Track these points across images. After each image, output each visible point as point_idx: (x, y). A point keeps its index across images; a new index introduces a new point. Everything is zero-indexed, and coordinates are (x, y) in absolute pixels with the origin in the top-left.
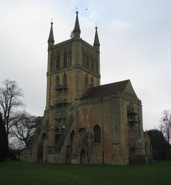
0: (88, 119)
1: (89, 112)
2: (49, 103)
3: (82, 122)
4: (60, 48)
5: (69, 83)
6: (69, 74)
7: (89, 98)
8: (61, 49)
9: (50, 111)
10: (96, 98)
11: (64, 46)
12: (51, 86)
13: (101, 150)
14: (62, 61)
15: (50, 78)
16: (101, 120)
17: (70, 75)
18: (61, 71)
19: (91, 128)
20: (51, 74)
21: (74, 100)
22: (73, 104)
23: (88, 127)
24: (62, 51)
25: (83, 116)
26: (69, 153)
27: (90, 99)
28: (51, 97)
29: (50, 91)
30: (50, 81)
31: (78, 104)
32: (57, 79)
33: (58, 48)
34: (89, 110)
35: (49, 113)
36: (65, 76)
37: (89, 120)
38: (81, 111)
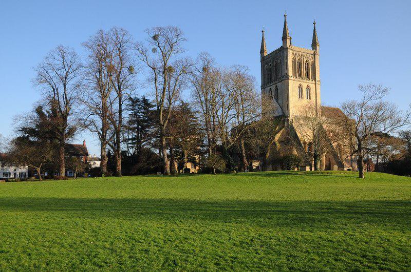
14: (303, 70)
36: (308, 88)
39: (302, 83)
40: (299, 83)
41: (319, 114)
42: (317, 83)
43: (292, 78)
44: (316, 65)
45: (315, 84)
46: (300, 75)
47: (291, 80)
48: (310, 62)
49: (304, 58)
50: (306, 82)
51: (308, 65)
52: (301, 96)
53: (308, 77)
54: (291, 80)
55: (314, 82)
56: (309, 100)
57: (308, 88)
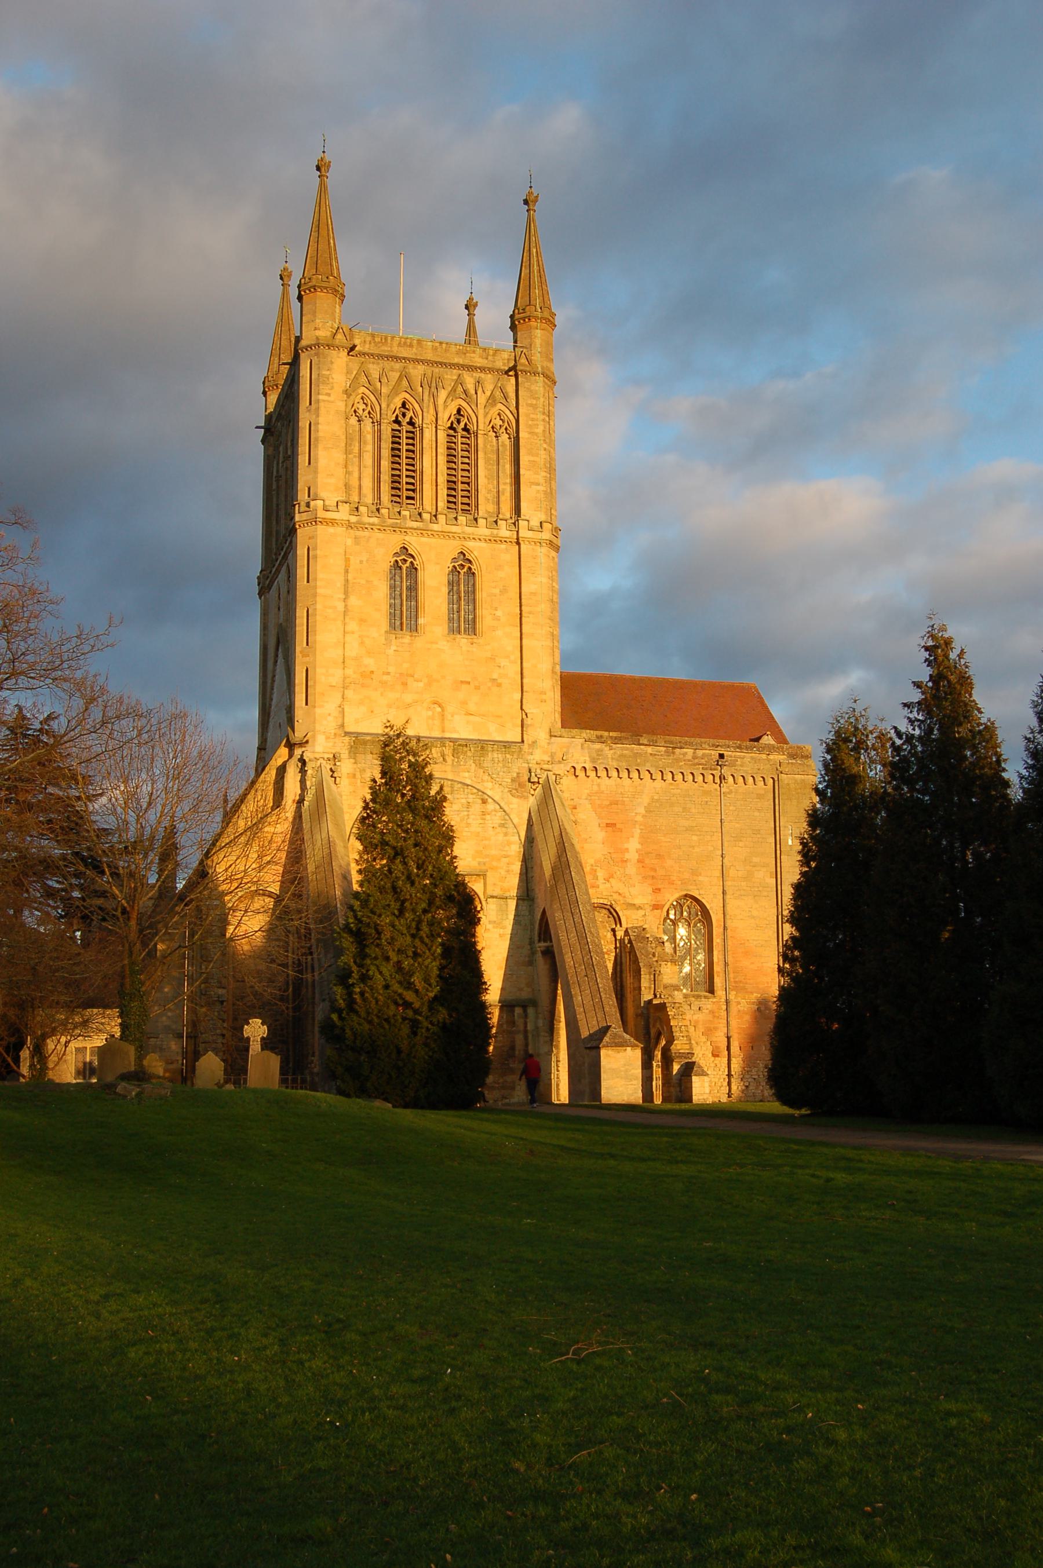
0: (632, 855)
1: (639, 818)
2: (343, 712)
3: (594, 872)
4: (417, 372)
5: (498, 619)
6: (499, 567)
8: (433, 385)
10: (690, 752)
11: (451, 375)
12: (353, 601)
13: (716, 1029)
14: (432, 465)
16: (718, 873)
18: (435, 527)
19: (656, 907)
20: (353, 519)
21: (542, 736)
22: (538, 756)
23: (637, 902)
24: (441, 401)
25: (600, 835)
26: (519, 1039)
30: (347, 571)
32: (396, 566)
33: (398, 366)
34: (642, 810)
37: (639, 861)
39: (416, 543)
40: (395, 541)
43: (343, 514)
47: (333, 522)
49: (443, 395)
52: (404, 614)
53: (461, 496)
54: (333, 522)
55: (504, 531)
56: (463, 640)
57: (463, 575)
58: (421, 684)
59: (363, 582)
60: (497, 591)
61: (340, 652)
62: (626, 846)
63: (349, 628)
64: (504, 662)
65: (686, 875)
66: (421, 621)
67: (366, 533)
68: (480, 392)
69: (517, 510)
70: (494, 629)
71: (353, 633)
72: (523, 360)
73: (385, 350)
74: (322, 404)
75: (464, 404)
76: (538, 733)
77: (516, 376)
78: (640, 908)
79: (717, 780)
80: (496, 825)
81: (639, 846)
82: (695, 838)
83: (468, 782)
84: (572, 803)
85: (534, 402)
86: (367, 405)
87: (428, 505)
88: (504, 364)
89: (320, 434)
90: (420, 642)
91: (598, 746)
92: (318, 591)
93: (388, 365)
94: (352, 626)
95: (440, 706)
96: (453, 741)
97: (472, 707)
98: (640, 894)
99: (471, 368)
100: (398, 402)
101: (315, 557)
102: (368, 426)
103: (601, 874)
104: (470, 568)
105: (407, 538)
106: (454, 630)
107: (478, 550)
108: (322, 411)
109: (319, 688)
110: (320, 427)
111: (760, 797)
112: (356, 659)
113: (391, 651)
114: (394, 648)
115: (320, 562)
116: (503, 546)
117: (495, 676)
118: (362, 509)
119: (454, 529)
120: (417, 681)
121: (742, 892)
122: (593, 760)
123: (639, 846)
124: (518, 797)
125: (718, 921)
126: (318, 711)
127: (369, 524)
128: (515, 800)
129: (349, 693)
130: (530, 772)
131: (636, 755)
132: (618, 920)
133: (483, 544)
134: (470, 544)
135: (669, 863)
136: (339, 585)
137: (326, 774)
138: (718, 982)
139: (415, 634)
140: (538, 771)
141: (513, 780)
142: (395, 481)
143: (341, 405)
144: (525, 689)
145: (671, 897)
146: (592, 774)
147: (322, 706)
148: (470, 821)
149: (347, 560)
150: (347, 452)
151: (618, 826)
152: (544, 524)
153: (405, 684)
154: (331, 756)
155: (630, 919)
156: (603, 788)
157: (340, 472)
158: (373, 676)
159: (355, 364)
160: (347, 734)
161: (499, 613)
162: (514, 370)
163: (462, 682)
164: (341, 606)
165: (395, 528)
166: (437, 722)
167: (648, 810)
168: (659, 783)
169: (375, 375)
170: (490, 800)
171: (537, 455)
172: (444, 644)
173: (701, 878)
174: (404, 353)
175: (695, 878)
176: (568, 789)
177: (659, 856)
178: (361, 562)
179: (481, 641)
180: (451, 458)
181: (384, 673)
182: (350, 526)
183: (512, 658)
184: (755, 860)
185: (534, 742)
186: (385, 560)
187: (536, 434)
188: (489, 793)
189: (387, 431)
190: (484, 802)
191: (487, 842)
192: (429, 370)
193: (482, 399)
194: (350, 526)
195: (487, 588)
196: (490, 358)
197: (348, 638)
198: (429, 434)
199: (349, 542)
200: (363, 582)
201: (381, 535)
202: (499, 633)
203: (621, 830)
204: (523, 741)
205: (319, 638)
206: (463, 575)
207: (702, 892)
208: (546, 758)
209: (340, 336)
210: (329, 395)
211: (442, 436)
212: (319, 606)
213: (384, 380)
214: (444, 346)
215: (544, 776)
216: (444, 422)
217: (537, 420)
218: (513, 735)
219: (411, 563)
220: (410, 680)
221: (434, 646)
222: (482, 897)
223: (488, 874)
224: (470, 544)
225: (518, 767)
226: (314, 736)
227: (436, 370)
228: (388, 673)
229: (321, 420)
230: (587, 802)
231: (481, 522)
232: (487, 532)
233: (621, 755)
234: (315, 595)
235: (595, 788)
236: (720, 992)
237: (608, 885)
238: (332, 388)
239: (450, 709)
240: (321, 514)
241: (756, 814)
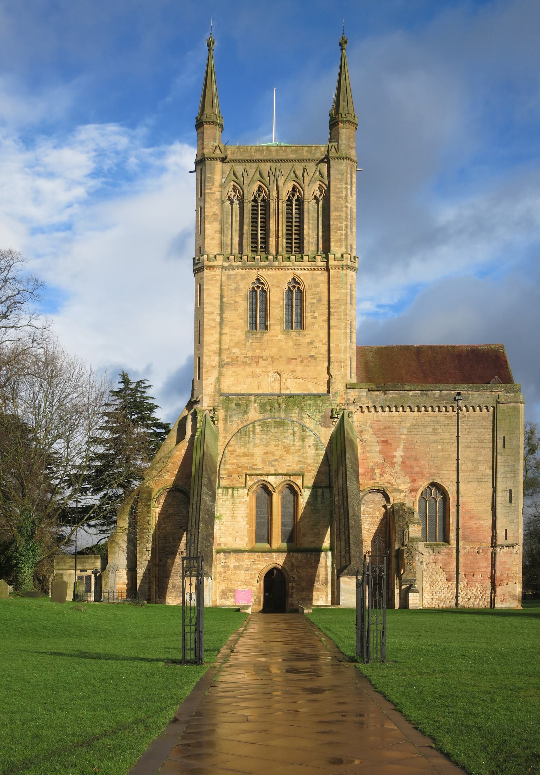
3: (373, 470)
4: (265, 167)
5: (315, 318)
6: (317, 286)
7: (408, 388)
8: (275, 175)
9: (221, 413)
11: (286, 167)
12: (227, 315)
13: (450, 564)
15: (221, 286)
17: (318, 290)
18: (276, 264)
20: (226, 264)
22: (338, 400)
23: (400, 488)
27: (411, 393)
28: (225, 357)
29: (221, 334)
30: (222, 297)
31: (360, 404)
32: (254, 291)
33: (254, 165)
34: (405, 431)
35: (221, 423)
37: (403, 462)
38: (371, 431)
39: (265, 274)
40: (253, 275)
41: (347, 371)
42: (331, 262)
43: (220, 262)
44: (332, 199)
45: (328, 270)
46: (260, 242)
47: (212, 268)
48: (311, 190)
49: (282, 180)
50: (285, 269)
51: (300, 202)
55: (320, 263)
56: (293, 333)
58: (267, 362)
59: (233, 302)
60: (315, 301)
61: (217, 346)
62: (394, 454)
63: (224, 331)
64: (319, 345)
65: (433, 471)
66: (268, 323)
67: (234, 272)
68: (305, 175)
69: (327, 250)
70: (313, 324)
71: (226, 334)
72: (333, 150)
73: (246, 156)
74: (207, 195)
75: (296, 184)
76: (339, 386)
77: (328, 162)
78: (402, 491)
79: (455, 410)
80: (311, 445)
81: (403, 454)
82: (439, 447)
83: (295, 419)
84: (360, 429)
85: (341, 177)
86: (236, 192)
87: (272, 250)
88: (322, 155)
89: (206, 214)
90: (267, 337)
91: (378, 393)
92: (205, 310)
93: (248, 165)
94: (226, 330)
95: (279, 374)
96: (286, 395)
97: (298, 374)
98: (403, 483)
99: (299, 161)
100: (255, 188)
101: (203, 290)
102: (236, 206)
103: (377, 471)
104: (298, 288)
105: (259, 273)
106: (289, 325)
107: (304, 276)
108: (207, 200)
109: (205, 370)
110: (206, 210)
111: (485, 419)
112: (228, 349)
113: (248, 344)
114: (250, 341)
115: (206, 293)
116: (319, 272)
117: (313, 354)
118: (232, 258)
119: (288, 264)
120: (264, 360)
121: (470, 480)
122: (374, 402)
123: (403, 454)
124: (325, 427)
125: (453, 498)
126: (205, 382)
127: (236, 266)
128: (323, 429)
129: (225, 370)
130: (332, 411)
131: (402, 397)
132: (388, 500)
133: (306, 272)
134: (298, 272)
135: (422, 462)
136: (217, 306)
137: (208, 418)
138: (452, 535)
139: (265, 331)
140: (338, 410)
141: (322, 417)
142: (254, 237)
143: (218, 195)
144: (331, 360)
145: (423, 484)
146: (372, 410)
147: (207, 379)
148: (295, 443)
149: (222, 290)
150: (222, 223)
151: (389, 442)
152: (345, 255)
153: (257, 362)
154: (212, 408)
155: (396, 498)
156: (380, 418)
157: (218, 235)
158: (239, 359)
159: (227, 167)
160: (221, 395)
161: (316, 314)
162: (327, 160)
163: (292, 359)
164: (218, 319)
165: (251, 268)
166: (277, 385)
167: (410, 431)
168: (416, 414)
169: (239, 174)
170: (307, 430)
171: (342, 211)
172: (280, 336)
173: (443, 472)
174: (258, 156)
175: (439, 472)
176: (356, 420)
177: (416, 459)
178: (231, 290)
179: (306, 332)
180: (289, 219)
181: (245, 357)
182: (223, 268)
183: (324, 341)
184: (480, 459)
185: (336, 393)
186: (246, 286)
187: (342, 198)
188: (307, 425)
189: (248, 206)
190: (304, 431)
191: (305, 455)
192: (273, 165)
193: (307, 179)
194: (223, 268)
195: (309, 299)
196: (313, 152)
197: (223, 337)
198: (273, 206)
199: (224, 279)
200: (233, 302)
201: (243, 272)
202: (316, 326)
203: (391, 444)
204: (329, 392)
205: (205, 339)
206: (295, 292)
207: (443, 480)
208: (343, 402)
209: (218, 151)
210: (211, 189)
211: (283, 206)
212: (205, 320)
213: (245, 175)
214: (283, 148)
215: (341, 413)
216: (284, 196)
217: (342, 188)
218: (323, 389)
219: (262, 287)
220: (260, 360)
221: (276, 338)
222: (301, 488)
223: (306, 474)
224: (298, 272)
225: (326, 409)
226: (202, 397)
227: (278, 164)
228: (247, 357)
229: (207, 205)
230: (369, 428)
231: (305, 258)
232: (309, 264)
233: (393, 398)
234: (203, 313)
235: (375, 419)
236: (453, 542)
237: (382, 478)
238: (213, 184)
239: (284, 376)
240: (206, 263)
241: (482, 430)
